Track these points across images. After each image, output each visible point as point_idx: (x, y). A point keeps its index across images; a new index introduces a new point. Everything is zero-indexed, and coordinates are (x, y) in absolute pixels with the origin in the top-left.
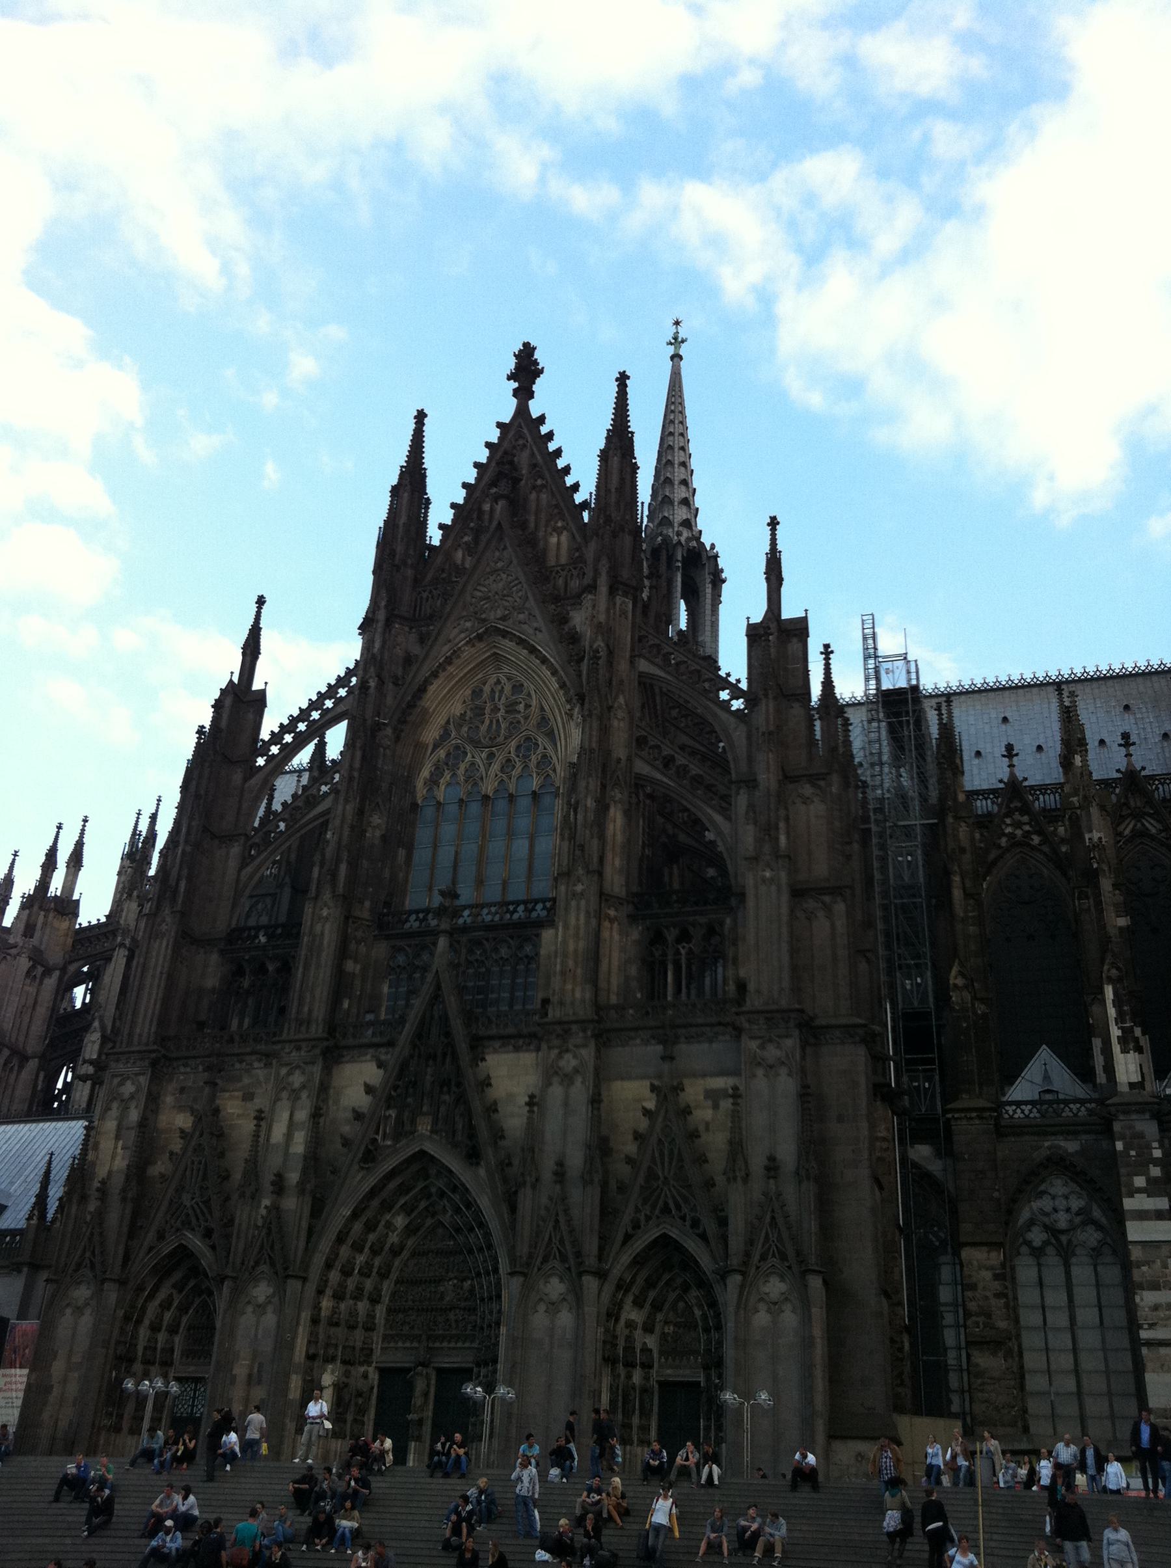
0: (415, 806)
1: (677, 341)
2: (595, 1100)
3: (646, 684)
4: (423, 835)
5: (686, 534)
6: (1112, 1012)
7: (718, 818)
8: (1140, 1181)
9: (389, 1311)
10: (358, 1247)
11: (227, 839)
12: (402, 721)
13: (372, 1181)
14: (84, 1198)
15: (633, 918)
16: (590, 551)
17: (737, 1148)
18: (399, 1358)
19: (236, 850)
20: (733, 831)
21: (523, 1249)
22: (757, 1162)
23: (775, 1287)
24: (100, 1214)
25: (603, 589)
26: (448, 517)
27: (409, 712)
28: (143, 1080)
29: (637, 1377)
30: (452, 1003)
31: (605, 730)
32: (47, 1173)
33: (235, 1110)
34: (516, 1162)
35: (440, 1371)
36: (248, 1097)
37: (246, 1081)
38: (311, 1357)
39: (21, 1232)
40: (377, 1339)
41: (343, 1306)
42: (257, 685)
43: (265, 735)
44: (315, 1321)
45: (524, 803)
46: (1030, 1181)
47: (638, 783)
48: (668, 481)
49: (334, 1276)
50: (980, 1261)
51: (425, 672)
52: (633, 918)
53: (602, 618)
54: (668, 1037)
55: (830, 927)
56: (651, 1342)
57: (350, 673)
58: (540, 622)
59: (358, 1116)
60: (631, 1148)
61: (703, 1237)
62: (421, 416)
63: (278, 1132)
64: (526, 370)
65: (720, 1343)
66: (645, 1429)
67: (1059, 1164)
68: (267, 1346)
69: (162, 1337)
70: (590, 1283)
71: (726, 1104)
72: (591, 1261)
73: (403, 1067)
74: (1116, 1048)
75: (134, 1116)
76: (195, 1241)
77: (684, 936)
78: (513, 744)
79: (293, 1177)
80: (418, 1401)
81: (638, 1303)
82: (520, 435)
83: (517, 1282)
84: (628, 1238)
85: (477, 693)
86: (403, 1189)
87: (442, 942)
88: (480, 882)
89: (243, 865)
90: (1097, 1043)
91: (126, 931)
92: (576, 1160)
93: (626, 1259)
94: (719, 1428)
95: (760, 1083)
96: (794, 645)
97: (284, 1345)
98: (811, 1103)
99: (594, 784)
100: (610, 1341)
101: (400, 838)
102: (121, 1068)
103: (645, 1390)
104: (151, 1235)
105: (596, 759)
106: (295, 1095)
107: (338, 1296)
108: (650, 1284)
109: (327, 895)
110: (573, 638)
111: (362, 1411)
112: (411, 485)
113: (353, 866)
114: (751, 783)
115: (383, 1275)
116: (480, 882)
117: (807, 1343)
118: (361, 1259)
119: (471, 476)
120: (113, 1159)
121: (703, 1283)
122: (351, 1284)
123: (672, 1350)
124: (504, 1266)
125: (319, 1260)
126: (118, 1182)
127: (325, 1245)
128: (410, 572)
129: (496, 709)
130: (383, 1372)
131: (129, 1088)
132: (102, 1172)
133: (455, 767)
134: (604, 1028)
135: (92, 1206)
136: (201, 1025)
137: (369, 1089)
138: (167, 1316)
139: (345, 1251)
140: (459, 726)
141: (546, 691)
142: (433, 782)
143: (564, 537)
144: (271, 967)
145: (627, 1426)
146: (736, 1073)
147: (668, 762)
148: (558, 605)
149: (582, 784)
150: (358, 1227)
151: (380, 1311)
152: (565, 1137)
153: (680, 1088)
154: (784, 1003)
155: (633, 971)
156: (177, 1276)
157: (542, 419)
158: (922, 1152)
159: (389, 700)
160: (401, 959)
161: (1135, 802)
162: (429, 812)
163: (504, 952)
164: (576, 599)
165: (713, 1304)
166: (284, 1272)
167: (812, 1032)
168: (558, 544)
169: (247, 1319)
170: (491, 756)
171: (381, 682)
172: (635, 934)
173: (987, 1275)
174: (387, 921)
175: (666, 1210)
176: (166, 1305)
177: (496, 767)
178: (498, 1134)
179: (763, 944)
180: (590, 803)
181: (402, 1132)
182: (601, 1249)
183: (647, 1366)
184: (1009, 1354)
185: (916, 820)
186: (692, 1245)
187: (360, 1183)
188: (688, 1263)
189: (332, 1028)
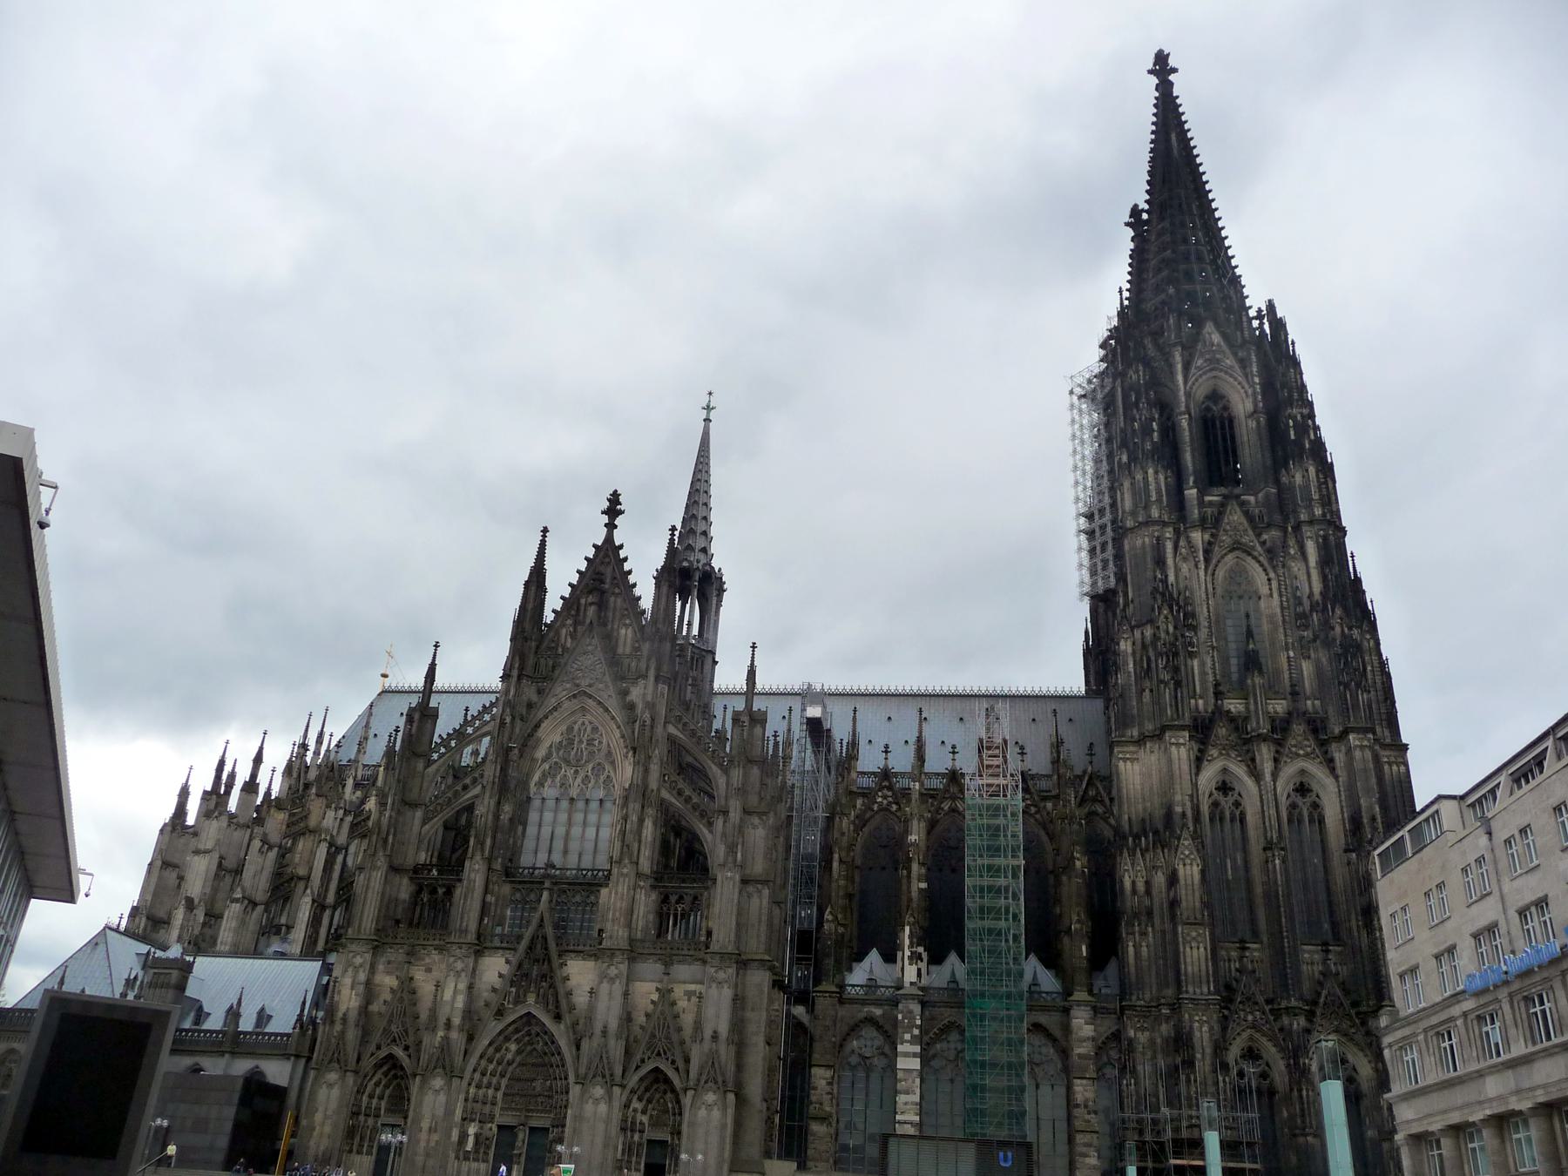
0: (529, 799)
1: (708, 408)
2: (626, 994)
3: (671, 740)
4: (533, 816)
5: (702, 557)
6: (907, 942)
7: (705, 831)
8: (907, 1037)
9: (505, 1094)
10: (490, 1061)
11: (414, 805)
12: (524, 745)
13: (500, 1027)
14: (333, 1022)
15: (653, 887)
16: (646, 647)
17: (698, 1026)
18: (508, 1120)
19: (419, 814)
20: (714, 842)
21: (582, 1070)
22: (708, 1033)
23: (710, 1097)
24: (343, 1032)
25: (652, 679)
26: (558, 605)
27: (529, 740)
28: (368, 956)
29: (636, 1137)
30: (549, 930)
31: (646, 771)
32: (304, 1003)
33: (424, 982)
34: (582, 1022)
35: (531, 1129)
36: (429, 970)
37: (427, 960)
38: (464, 1119)
39: (288, 1035)
40: (497, 1111)
41: (481, 1092)
42: (433, 704)
43: (436, 739)
44: (466, 1100)
45: (594, 805)
46: (854, 1029)
47: (663, 807)
48: (694, 516)
49: (477, 1076)
50: (820, 1077)
51: (540, 715)
52: (653, 887)
53: (649, 698)
54: (667, 964)
55: (760, 902)
56: (645, 1119)
57: (492, 705)
58: (611, 691)
59: (494, 990)
60: (642, 1019)
61: (677, 1069)
62: (545, 530)
63: (448, 995)
64: (613, 509)
65: (680, 1124)
66: (638, 1163)
67: (870, 1020)
68: (440, 1112)
69: (375, 1101)
70: (617, 1090)
71: (694, 999)
72: (618, 1079)
73: (520, 966)
74: (906, 961)
75: (362, 977)
76: (399, 1052)
77: (680, 900)
78: (590, 766)
79: (457, 1021)
80: (519, 1144)
81: (640, 1099)
82: (607, 555)
83: (578, 1087)
84: (637, 1067)
85: (570, 729)
86: (517, 1031)
87: (545, 894)
88: (566, 852)
89: (424, 823)
90: (899, 954)
91: (327, 831)
92: (613, 1025)
93: (636, 1078)
94: (676, 1165)
95: (714, 991)
96: (758, 730)
97: (449, 1112)
98: (739, 1001)
99: (638, 806)
100: (624, 1121)
101: (520, 819)
102: (353, 947)
103: (640, 1144)
104: (372, 1048)
105: (640, 792)
106: (458, 974)
107: (478, 1087)
108: (647, 1090)
109: (478, 857)
110: (631, 707)
111: (488, 1147)
112: (536, 581)
113: (494, 838)
114: (725, 813)
115: (502, 1076)
116: (566, 852)
117: (724, 1126)
118: (491, 1067)
119: (575, 579)
120: (348, 999)
121: (673, 1091)
122: (485, 1080)
123: (655, 1123)
124: (572, 1079)
125: (470, 1068)
126: (353, 1015)
127: (473, 1061)
128: (534, 644)
129: (581, 742)
130: (500, 1127)
131: (358, 960)
132: (342, 1008)
133: (555, 776)
134: (633, 953)
135: (338, 1027)
136: (398, 922)
137: (501, 976)
138: (378, 1091)
139: (483, 1063)
140: (558, 749)
141: (613, 737)
142: (541, 784)
143: (630, 631)
144: (441, 891)
145: (629, 1162)
146: (702, 983)
147: (680, 793)
148: (622, 676)
149: (631, 806)
150: (491, 1050)
151: (500, 1095)
152: (608, 1012)
153: (671, 991)
154: (730, 949)
155: (651, 917)
156: (385, 1068)
157: (621, 547)
158: (799, 1011)
159: (517, 730)
160: (518, 896)
161: (954, 789)
162: (536, 803)
163: (578, 898)
164: (635, 681)
165: (678, 1102)
166: (451, 1073)
167: (743, 963)
168: (626, 634)
169: (429, 1098)
170: (576, 772)
171: (513, 718)
172: (654, 896)
173: (824, 1082)
174: (509, 873)
175: (659, 1054)
176: (377, 1084)
177: (579, 780)
178: (572, 1008)
179: (725, 907)
180: (635, 818)
181: (518, 1001)
182: (624, 1071)
183: (642, 1131)
184: (830, 1124)
185: (821, 814)
186: (671, 1074)
187: (494, 1027)
188: (667, 1081)
189: (478, 938)
